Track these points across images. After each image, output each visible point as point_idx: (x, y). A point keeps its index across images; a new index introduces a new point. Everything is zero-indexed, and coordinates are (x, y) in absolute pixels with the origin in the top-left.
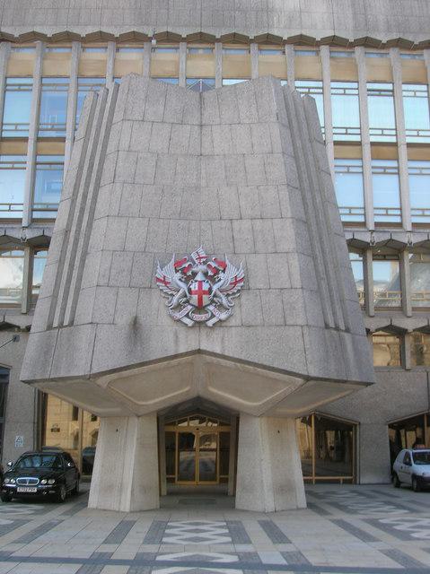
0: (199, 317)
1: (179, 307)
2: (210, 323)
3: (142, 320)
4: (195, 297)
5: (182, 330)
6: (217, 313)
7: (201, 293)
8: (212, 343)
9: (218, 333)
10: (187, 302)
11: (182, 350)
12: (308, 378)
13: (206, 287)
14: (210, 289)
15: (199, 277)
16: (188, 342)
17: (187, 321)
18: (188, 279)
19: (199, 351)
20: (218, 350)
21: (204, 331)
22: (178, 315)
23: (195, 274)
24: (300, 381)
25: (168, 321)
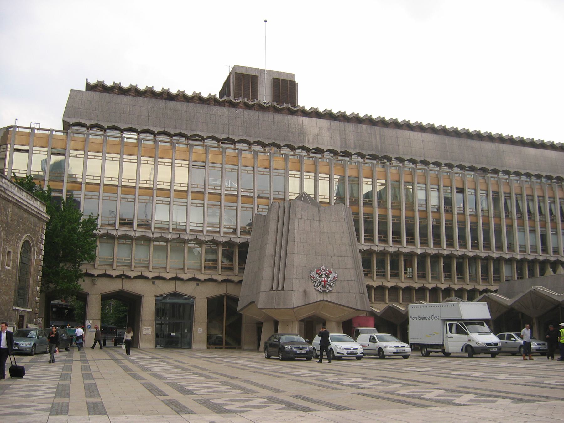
0: (324, 289)
1: (318, 286)
2: (327, 291)
3: (307, 290)
4: (323, 283)
5: (318, 293)
6: (329, 288)
7: (325, 281)
8: (328, 298)
9: (329, 295)
10: (320, 284)
11: (319, 300)
12: (356, 310)
13: (326, 279)
14: (327, 281)
15: (324, 276)
16: (320, 298)
17: (320, 290)
18: (320, 276)
19: (324, 300)
20: (329, 300)
21: (325, 294)
22: (318, 288)
23: (322, 275)
24: (354, 310)
25: (314, 290)
